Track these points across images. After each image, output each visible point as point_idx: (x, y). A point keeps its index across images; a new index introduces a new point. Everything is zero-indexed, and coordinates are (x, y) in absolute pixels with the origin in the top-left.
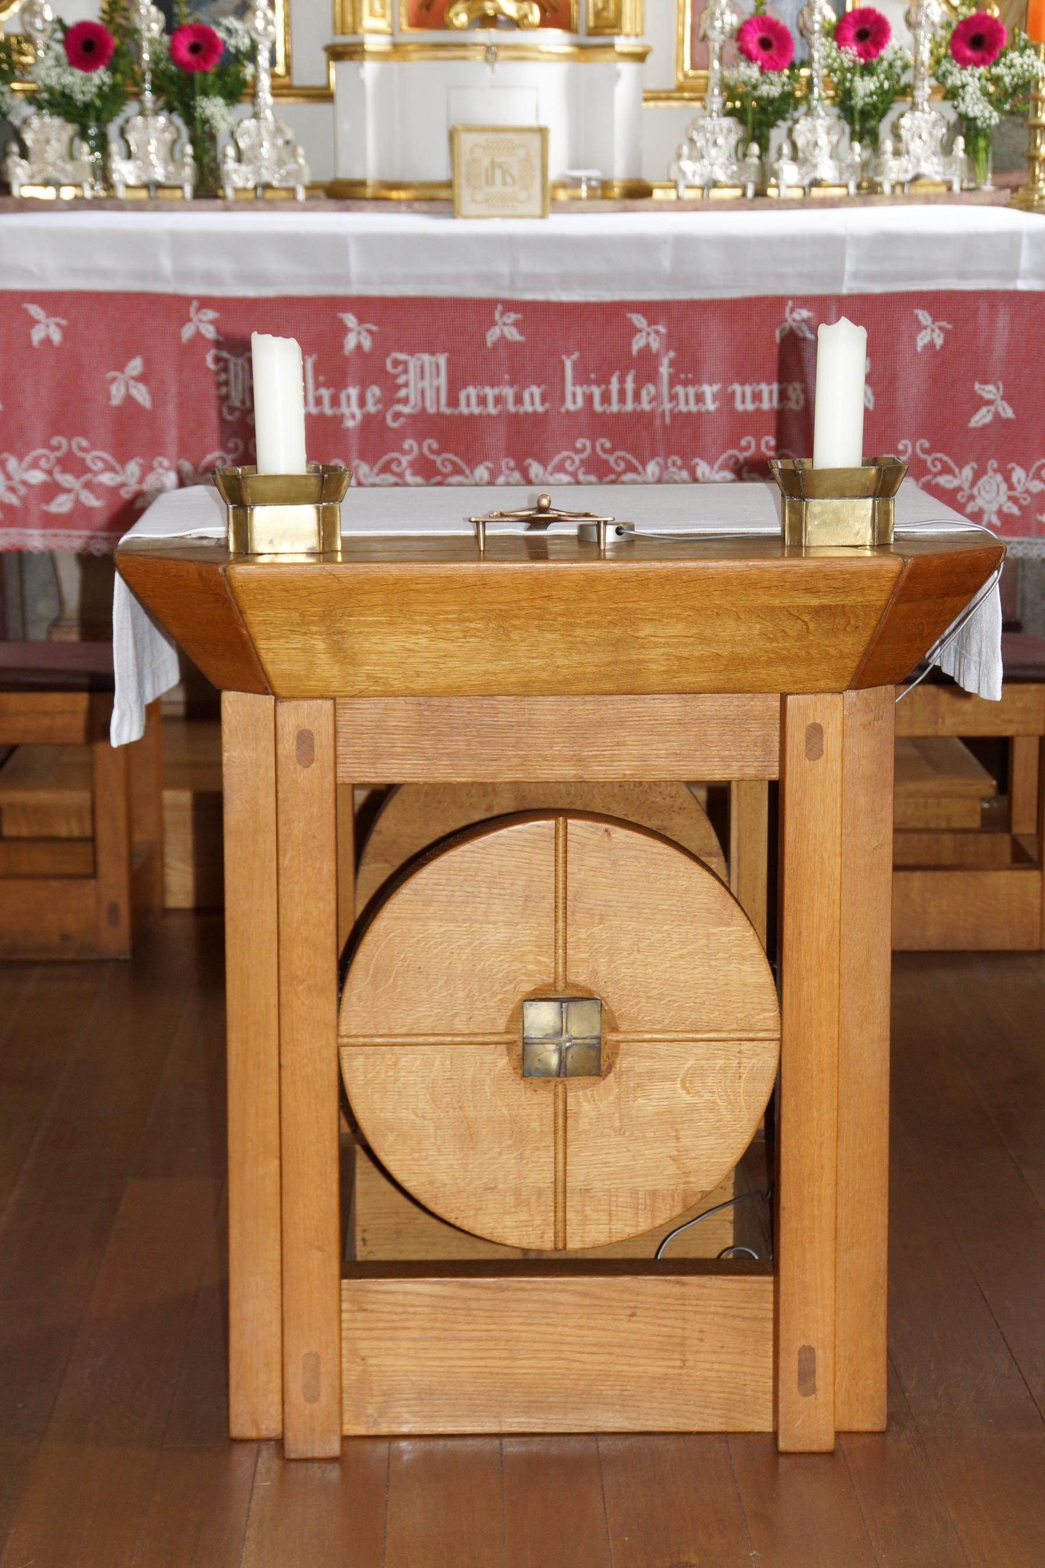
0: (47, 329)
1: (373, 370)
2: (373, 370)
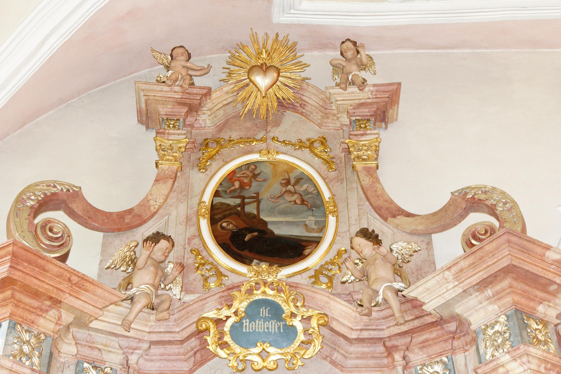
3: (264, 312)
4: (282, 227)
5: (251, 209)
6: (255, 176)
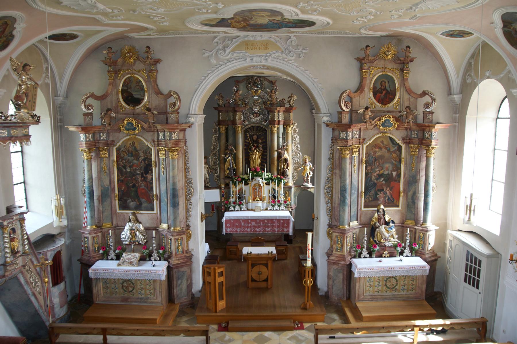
0: (232, 221)
1: (250, 223)
2: (250, 223)
3: (130, 125)
4: (136, 96)
5: (129, 90)
6: (130, 81)
